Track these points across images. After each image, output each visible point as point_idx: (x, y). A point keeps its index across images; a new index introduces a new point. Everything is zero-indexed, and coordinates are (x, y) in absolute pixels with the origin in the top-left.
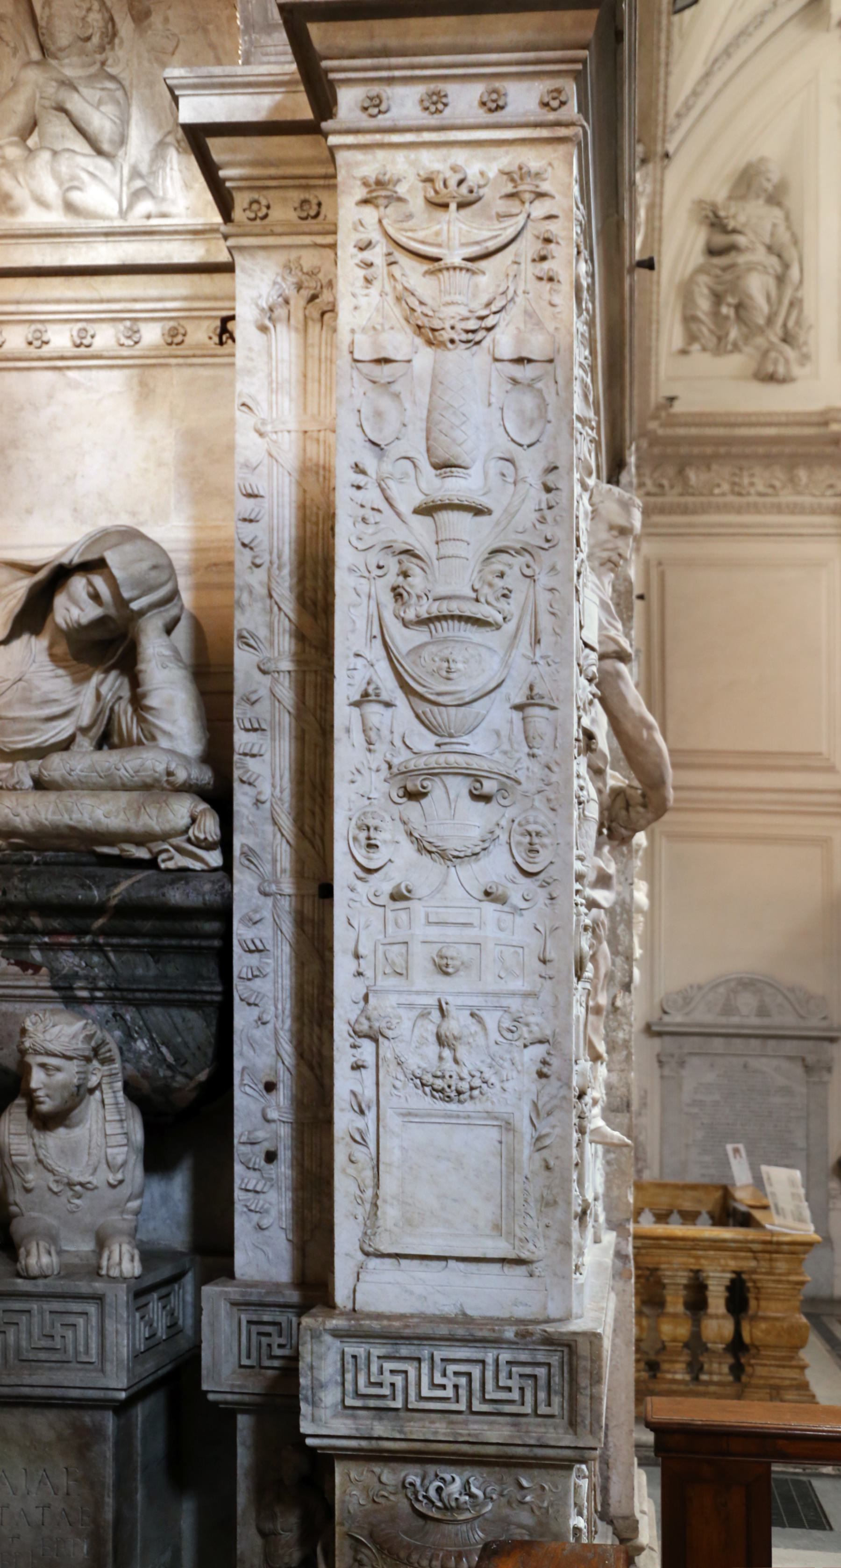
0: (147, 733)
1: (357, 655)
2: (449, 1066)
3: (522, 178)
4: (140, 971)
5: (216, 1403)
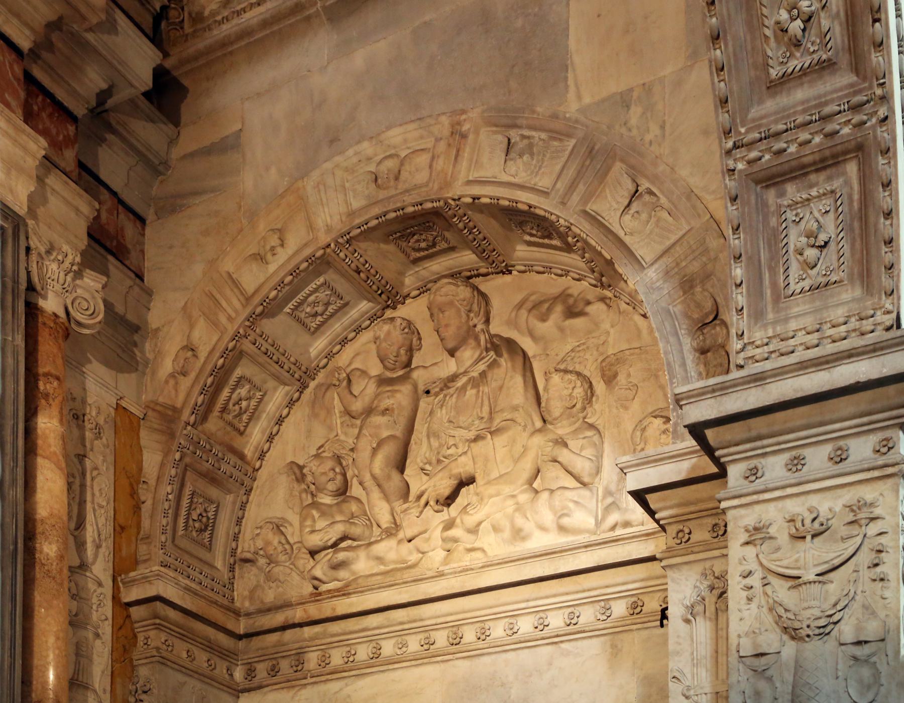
3: (859, 508)
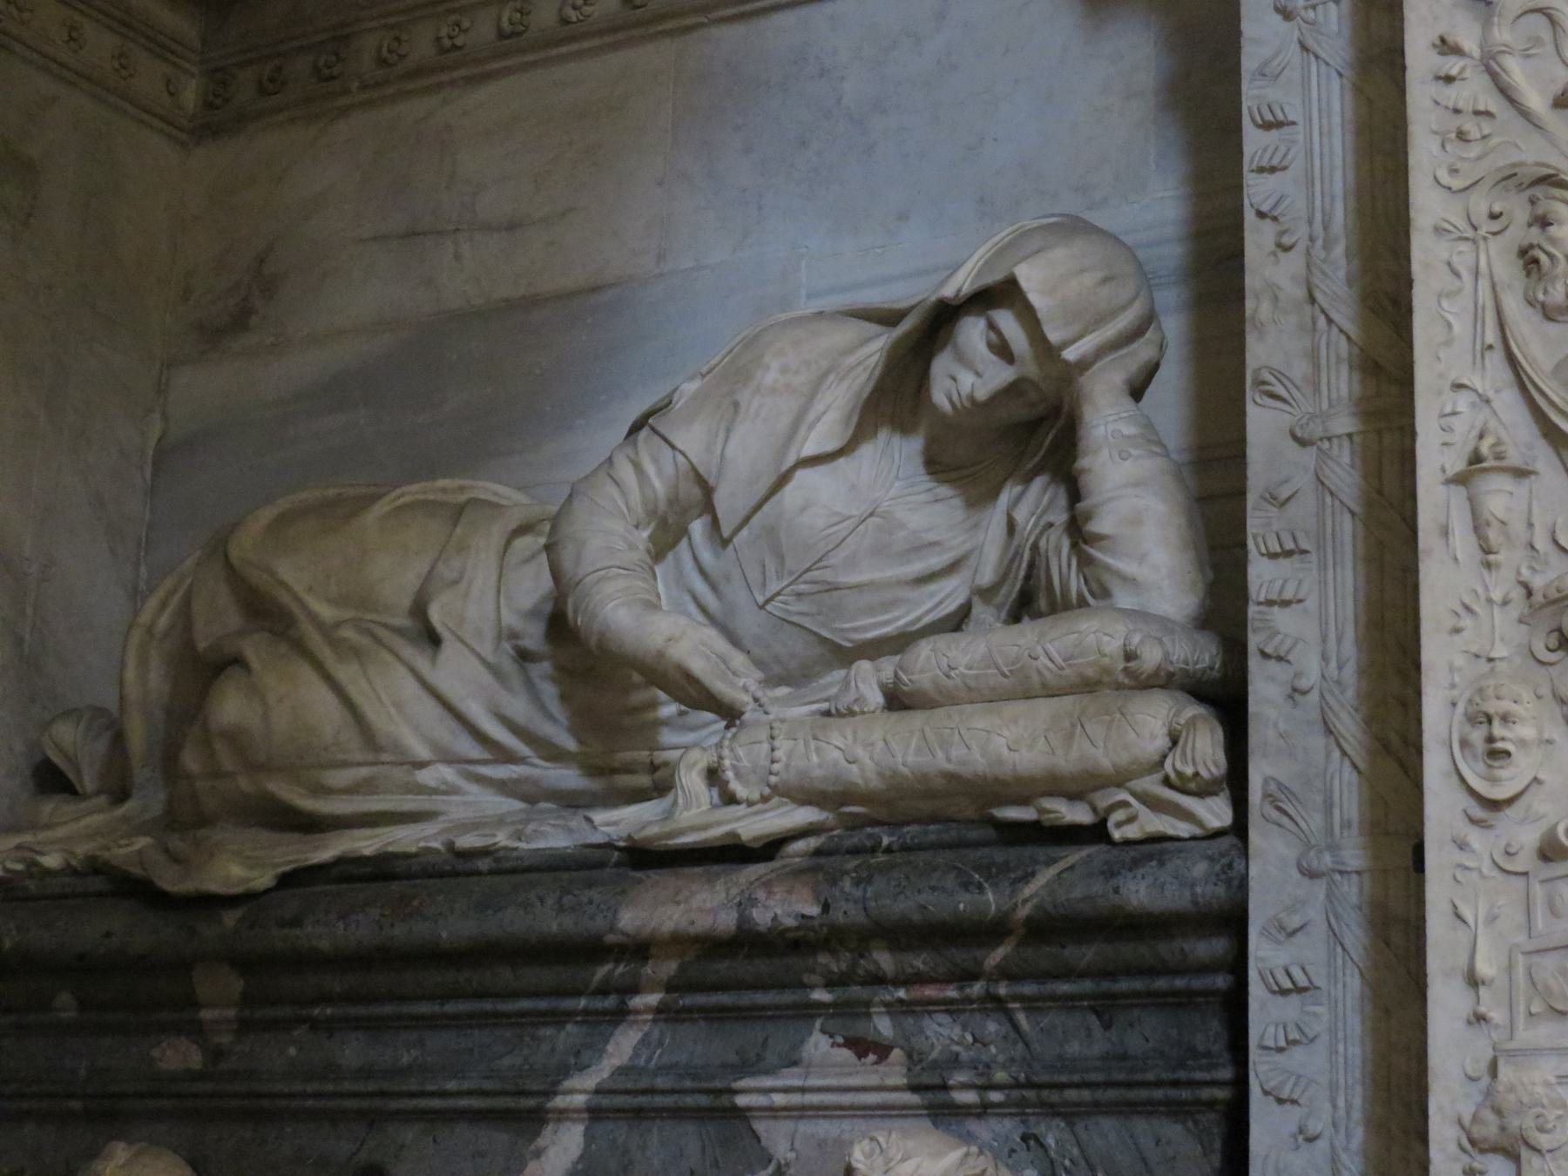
0: (1094, 586)
1: (1459, 387)
4: (1074, 1048)
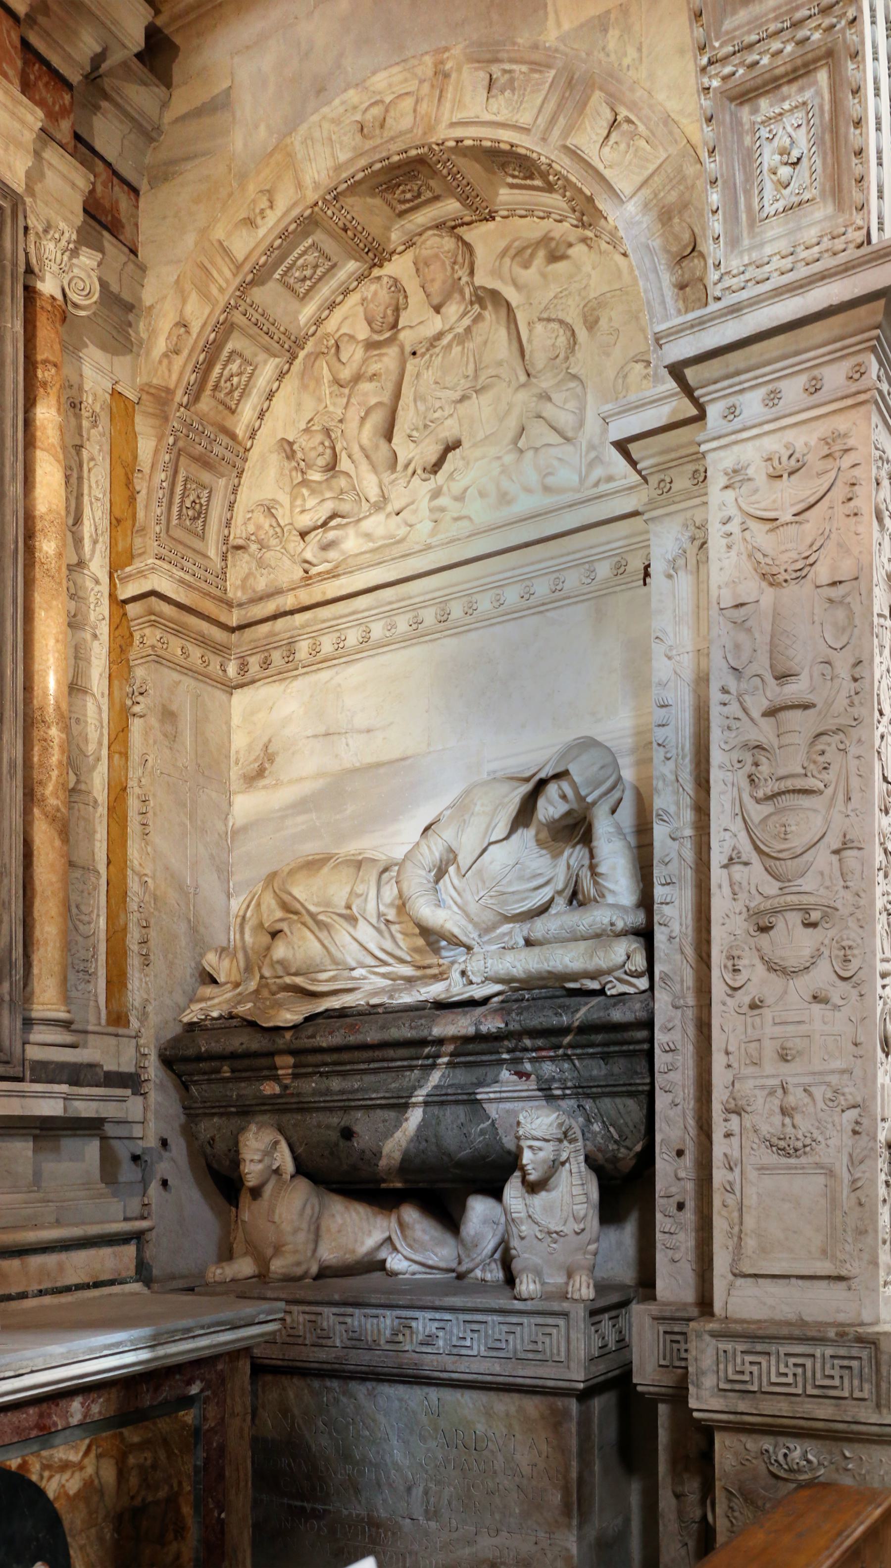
2: (789, 1130)
4: (595, 1072)
5: (643, 1394)
